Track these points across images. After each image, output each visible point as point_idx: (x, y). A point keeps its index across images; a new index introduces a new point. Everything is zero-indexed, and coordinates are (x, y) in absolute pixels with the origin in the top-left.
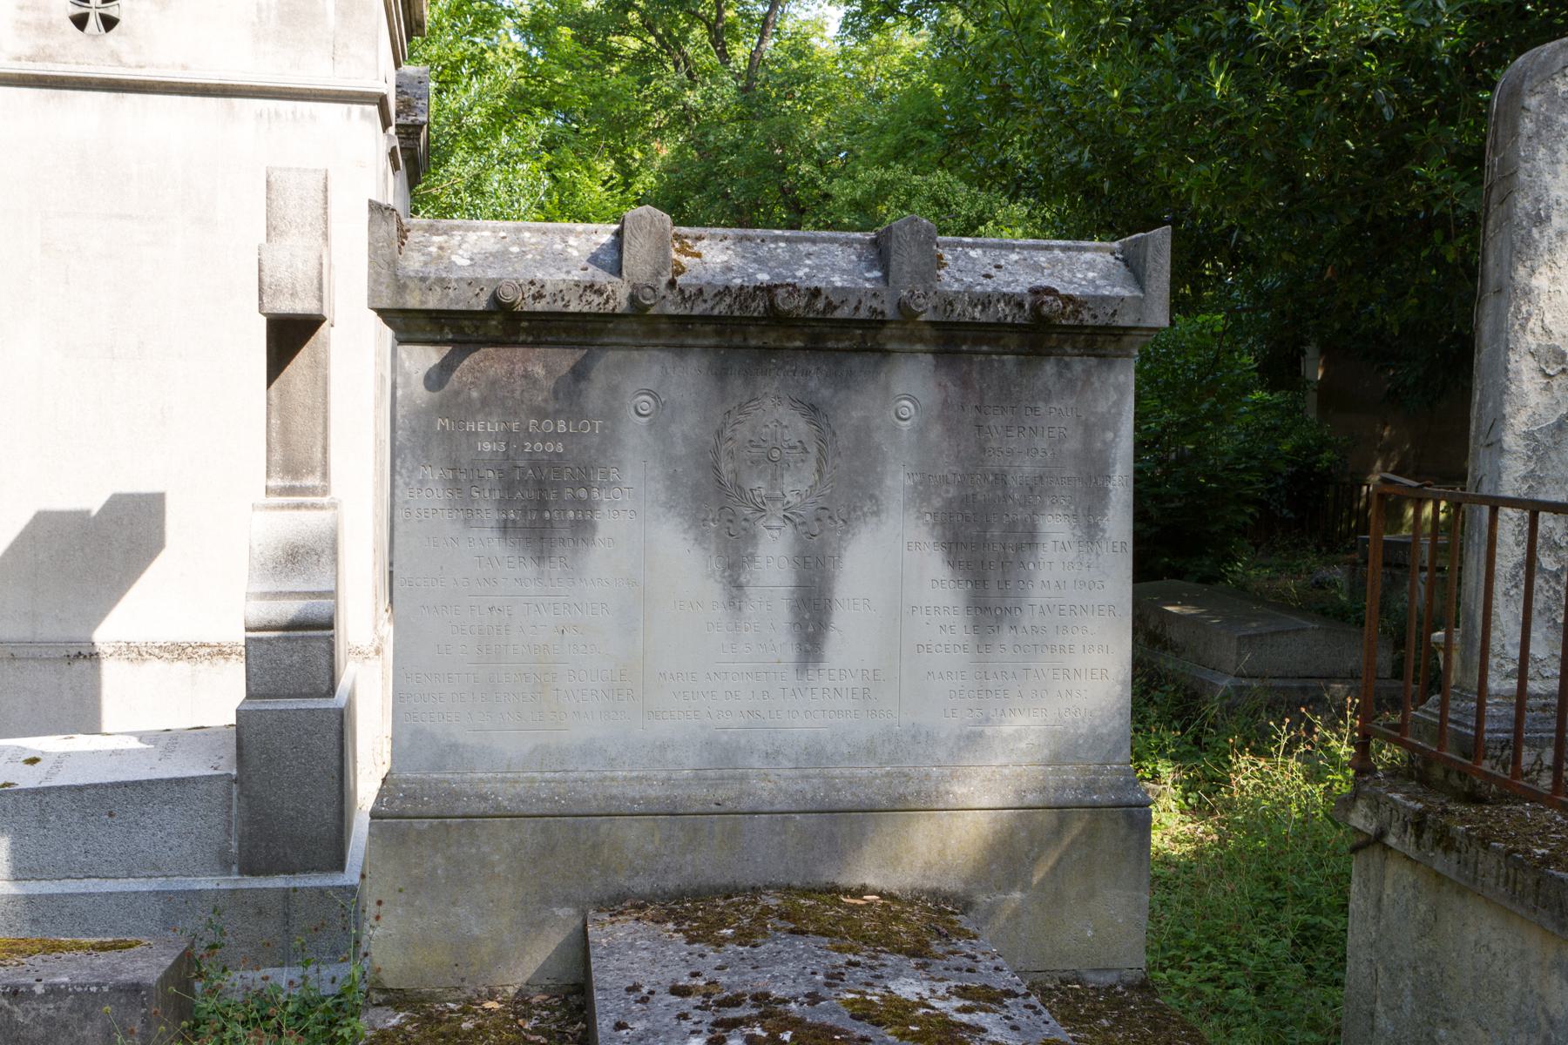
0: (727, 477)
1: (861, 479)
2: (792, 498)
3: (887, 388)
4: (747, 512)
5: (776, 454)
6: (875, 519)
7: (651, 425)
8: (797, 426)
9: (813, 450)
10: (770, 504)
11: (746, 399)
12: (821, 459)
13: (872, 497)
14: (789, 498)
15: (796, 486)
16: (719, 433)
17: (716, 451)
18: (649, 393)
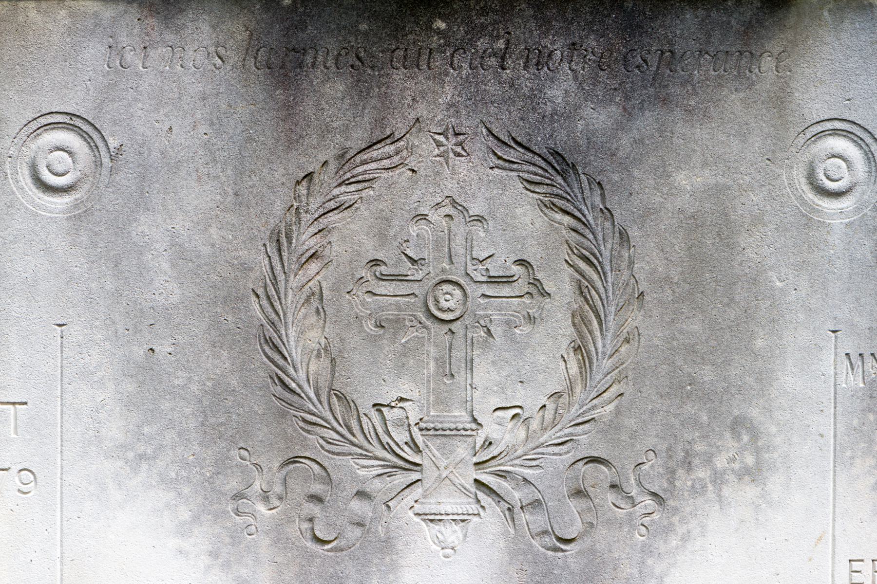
0: (306, 369)
1: (707, 374)
2: (502, 432)
3: (780, 102)
4: (366, 471)
5: (450, 299)
6: (750, 491)
7: (79, 217)
8: (516, 219)
9: (561, 286)
10: (432, 447)
11: (357, 139)
12: (588, 313)
13: (738, 425)
14: (490, 429)
15: (513, 386)
16: (280, 240)
17: (270, 294)
18: (72, 122)
